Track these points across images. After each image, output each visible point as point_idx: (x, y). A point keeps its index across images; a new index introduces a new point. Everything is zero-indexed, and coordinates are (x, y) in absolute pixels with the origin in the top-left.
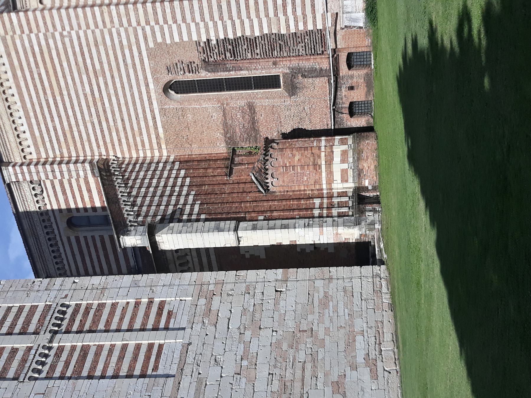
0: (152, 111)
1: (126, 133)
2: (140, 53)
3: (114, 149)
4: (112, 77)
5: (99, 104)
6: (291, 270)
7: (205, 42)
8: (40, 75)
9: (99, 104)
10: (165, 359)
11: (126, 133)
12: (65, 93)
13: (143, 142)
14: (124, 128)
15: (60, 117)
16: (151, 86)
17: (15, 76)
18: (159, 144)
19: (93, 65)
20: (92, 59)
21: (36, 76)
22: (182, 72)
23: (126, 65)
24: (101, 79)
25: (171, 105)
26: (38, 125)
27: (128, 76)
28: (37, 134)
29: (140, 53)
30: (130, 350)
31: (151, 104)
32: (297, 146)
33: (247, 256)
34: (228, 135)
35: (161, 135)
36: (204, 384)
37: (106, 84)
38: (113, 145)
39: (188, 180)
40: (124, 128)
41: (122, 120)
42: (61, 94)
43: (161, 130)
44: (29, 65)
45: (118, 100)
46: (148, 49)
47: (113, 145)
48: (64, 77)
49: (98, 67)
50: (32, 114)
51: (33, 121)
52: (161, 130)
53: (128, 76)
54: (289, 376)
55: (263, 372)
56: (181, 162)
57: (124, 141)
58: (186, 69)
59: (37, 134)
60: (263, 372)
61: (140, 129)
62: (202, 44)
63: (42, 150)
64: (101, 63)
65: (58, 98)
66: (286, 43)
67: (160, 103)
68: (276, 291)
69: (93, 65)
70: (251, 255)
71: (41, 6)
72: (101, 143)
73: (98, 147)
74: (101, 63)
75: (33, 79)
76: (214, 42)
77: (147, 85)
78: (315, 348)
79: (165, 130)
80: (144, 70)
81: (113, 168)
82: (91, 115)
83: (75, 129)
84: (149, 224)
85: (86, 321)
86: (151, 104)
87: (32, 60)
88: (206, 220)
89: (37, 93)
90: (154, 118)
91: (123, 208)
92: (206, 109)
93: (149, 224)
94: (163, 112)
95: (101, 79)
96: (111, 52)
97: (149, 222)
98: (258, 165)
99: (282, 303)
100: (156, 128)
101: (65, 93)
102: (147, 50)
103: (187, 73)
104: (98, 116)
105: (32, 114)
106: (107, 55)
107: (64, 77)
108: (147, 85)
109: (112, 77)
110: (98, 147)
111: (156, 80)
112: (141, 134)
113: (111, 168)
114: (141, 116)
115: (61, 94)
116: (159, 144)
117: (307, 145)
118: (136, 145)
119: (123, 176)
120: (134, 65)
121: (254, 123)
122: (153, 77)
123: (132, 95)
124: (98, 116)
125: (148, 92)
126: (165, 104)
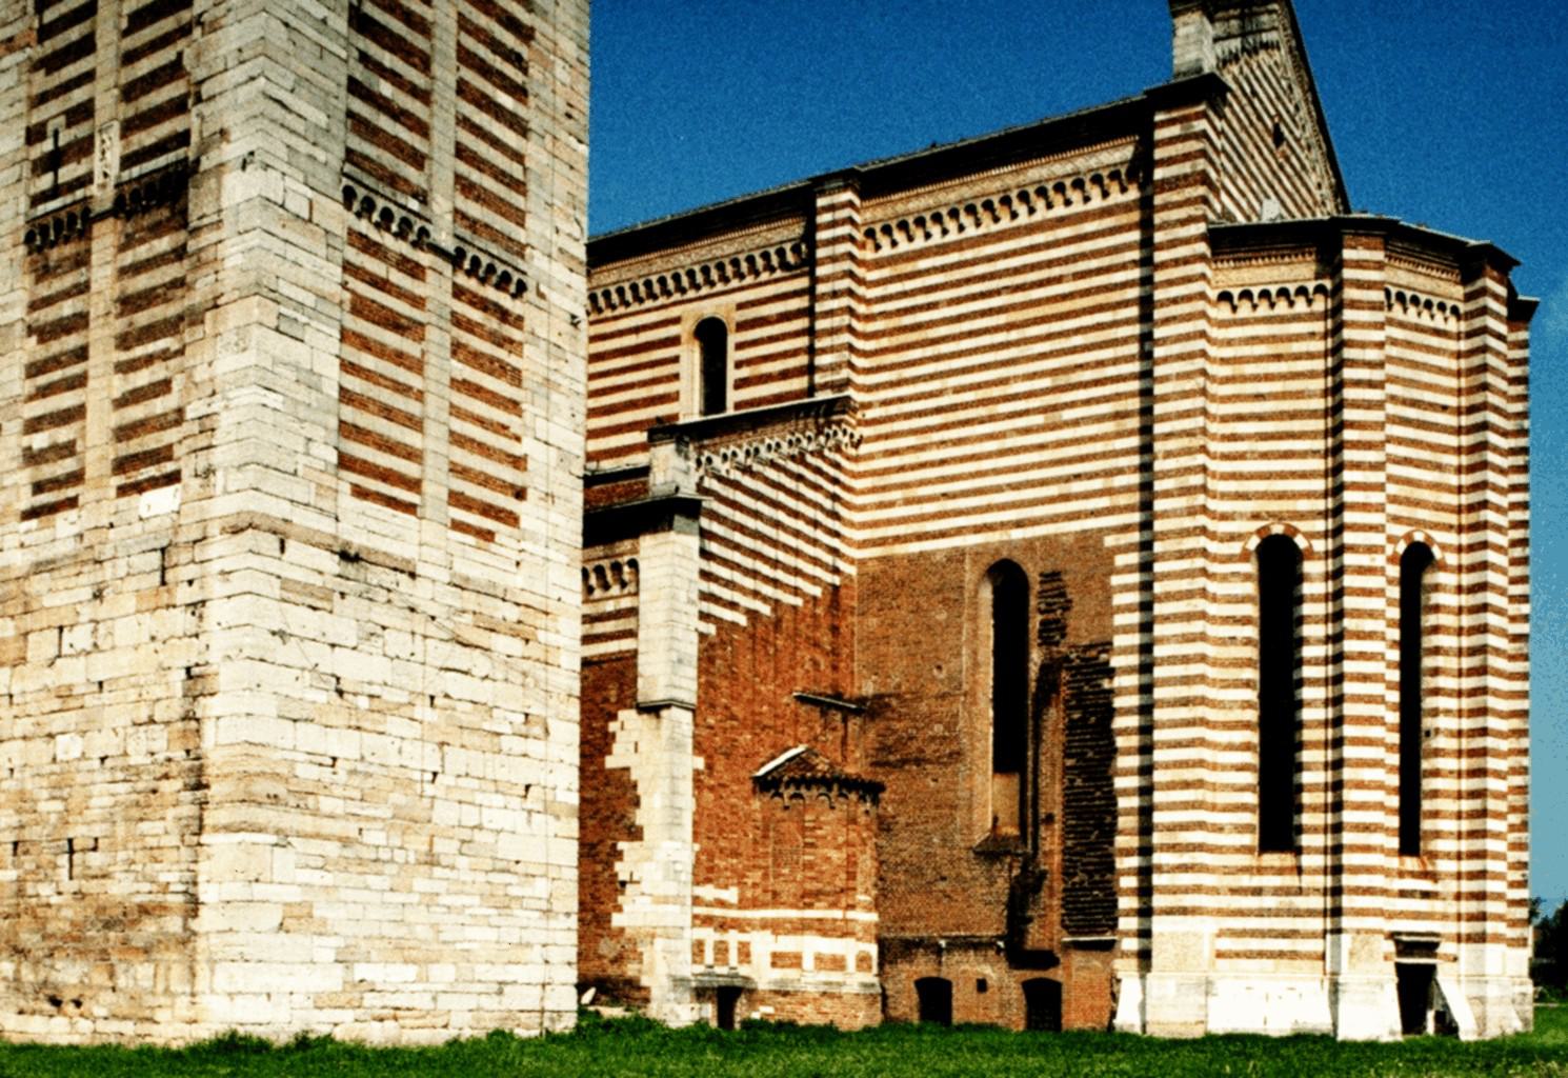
0: (959, 531)
1: (913, 467)
2: (1094, 513)
3: (878, 438)
4: (1042, 447)
5: (982, 411)
6: (574, 824)
7: (1107, 662)
8: (1059, 280)
9: (982, 411)
10: (379, 515)
11: (913, 467)
12: (1014, 335)
13: (891, 504)
14: (923, 465)
15: (959, 319)
16: (1017, 534)
17: (1061, 222)
18: (882, 542)
19: (1072, 405)
20: (1087, 402)
21: (1056, 271)
22: (1043, 606)
23: (1067, 479)
24: (1039, 419)
25: (970, 574)
26: (943, 269)
27: (1043, 483)
28: (923, 264)
29: (1094, 513)
30: (410, 438)
31: (978, 529)
32: (861, 858)
33: (613, 726)
34: (894, 702)
35: (900, 549)
36: (318, 604)
37: (1027, 431)
38: (887, 437)
39: (799, 602)
40: (923, 465)
41: (943, 462)
42: (1010, 327)
43: (915, 548)
44: (1084, 256)
45: (989, 455)
46: (1102, 531)
47: (887, 437)
48: (1049, 337)
49: (1068, 415)
50: (969, 254)
51: (954, 257)
52: (915, 548)
53: (1043, 483)
54: (327, 804)
55: (345, 745)
56: (836, 588)
57: (895, 461)
58: (1051, 616)
59: (923, 264)
60: (345, 745)
61: (920, 500)
62: (1104, 656)
63: (886, 272)
64: (1076, 423)
65: (1001, 319)
66: (1091, 847)
67: (978, 552)
68: (528, 787)
69: (1072, 405)
70: (613, 736)
71: (1213, 294)
72: (893, 410)
73: (885, 403)
74: (1076, 423)
75: (1050, 264)
76: (1106, 684)
77: (1019, 524)
78: (391, 869)
79: (912, 559)
80: (1054, 519)
81: (835, 433)
82: (958, 390)
83: (930, 351)
84: (699, 502)
85: (481, 337)
86: (978, 529)
87: (1094, 264)
88: (703, 636)
89: (1017, 271)
90: (943, 534)
91: (740, 447)
92: (959, 655)
93: (699, 502)
94: (957, 556)
95: (1039, 419)
96: (1099, 447)
97: (704, 504)
98: (822, 766)
99: (499, 800)
100: (920, 537)
101: (1014, 335)
102: (1100, 530)
103: (1039, 618)
104: (954, 408)
105: (969, 254)
106: (1093, 439)
107: (1049, 337)
108: (1019, 524)
109: (1042, 447)
110: (885, 403)
111: (1029, 545)
112: (908, 502)
113: (834, 427)
114: (950, 505)
115: (1010, 327)
116: (882, 542)
117: (860, 878)
118: (884, 489)
119: (812, 453)
120: (1065, 498)
121: (918, 762)
122: (1038, 539)
123: (998, 489)
124: (954, 408)
125: (1003, 525)
126: (975, 562)
